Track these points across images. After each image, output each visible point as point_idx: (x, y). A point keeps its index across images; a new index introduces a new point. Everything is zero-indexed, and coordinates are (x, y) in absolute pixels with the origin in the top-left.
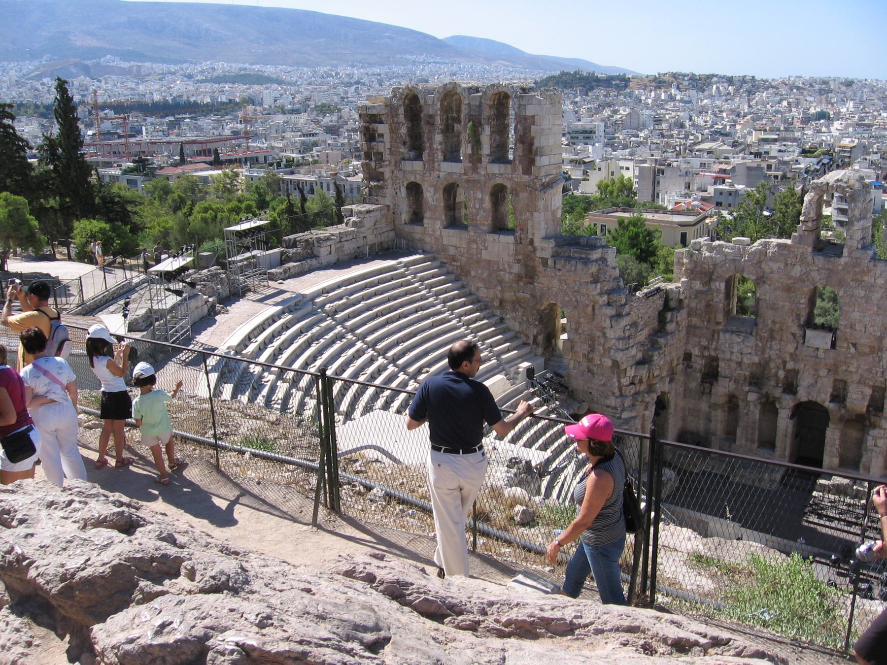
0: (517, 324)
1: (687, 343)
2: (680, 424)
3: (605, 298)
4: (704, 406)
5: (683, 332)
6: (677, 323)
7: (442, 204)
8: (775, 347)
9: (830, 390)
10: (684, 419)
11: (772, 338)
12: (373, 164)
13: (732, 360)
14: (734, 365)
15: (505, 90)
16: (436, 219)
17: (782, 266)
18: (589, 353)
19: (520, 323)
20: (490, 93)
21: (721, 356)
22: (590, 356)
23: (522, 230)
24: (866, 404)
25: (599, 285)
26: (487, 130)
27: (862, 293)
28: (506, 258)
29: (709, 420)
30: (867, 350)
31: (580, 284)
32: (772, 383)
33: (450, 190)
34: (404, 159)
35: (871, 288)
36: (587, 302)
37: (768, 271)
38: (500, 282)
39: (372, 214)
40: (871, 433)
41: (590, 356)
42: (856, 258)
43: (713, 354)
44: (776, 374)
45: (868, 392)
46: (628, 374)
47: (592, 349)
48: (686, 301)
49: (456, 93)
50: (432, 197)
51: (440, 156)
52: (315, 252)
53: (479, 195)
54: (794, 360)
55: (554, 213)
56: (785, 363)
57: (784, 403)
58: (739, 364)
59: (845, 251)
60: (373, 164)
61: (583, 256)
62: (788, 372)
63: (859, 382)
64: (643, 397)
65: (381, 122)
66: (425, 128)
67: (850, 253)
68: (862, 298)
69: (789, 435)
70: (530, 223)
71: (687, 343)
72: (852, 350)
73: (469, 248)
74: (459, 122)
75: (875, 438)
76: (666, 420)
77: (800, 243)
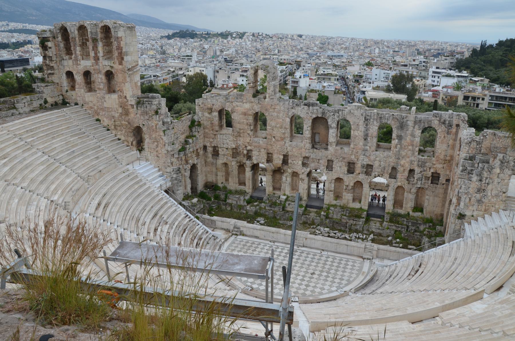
0: (123, 136)
1: (204, 141)
2: (204, 178)
3: (161, 122)
4: (214, 170)
5: (202, 136)
6: (198, 132)
7: (84, 81)
9: (266, 157)
10: (206, 176)
12: (48, 62)
13: (223, 147)
14: (225, 150)
15: (107, 24)
16: (81, 88)
19: (124, 136)
20: (100, 26)
21: (219, 146)
23: (121, 92)
24: (281, 162)
25: (158, 116)
26: (100, 45)
27: (276, 114)
28: (115, 106)
29: (217, 175)
30: (279, 139)
32: (242, 156)
33: (87, 74)
34: (63, 59)
35: (279, 112)
36: (153, 124)
38: (113, 117)
39: (49, 87)
43: (216, 145)
44: (243, 152)
45: (282, 157)
46: (175, 156)
47: (157, 146)
48: (202, 122)
49: (85, 27)
50: (79, 78)
51: (80, 57)
52: (16, 107)
53: (100, 76)
54: (250, 146)
55: (136, 83)
56: (246, 147)
57: (247, 164)
58: (227, 149)
59: (267, 96)
60: (48, 62)
62: (248, 151)
64: (183, 167)
65: (49, 41)
66: (72, 44)
70: (124, 89)
71: (204, 141)
72: (274, 140)
73: (98, 101)
74: (88, 41)
75: (286, 177)
76: (197, 176)
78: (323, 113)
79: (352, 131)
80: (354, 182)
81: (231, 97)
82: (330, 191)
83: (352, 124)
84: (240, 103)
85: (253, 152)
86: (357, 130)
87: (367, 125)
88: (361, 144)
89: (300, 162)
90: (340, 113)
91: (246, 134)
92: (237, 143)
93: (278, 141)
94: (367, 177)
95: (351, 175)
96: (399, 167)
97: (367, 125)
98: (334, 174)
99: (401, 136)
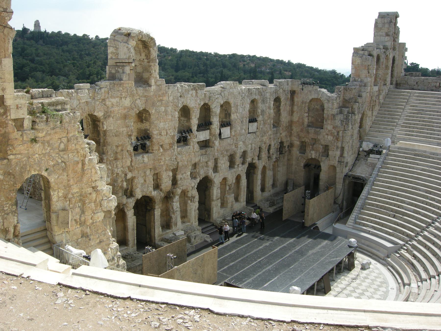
8: (119, 166)
11: (116, 159)
17: (118, 99)
18: (80, 216)
22: (83, 219)
31: (68, 141)
36: (76, 159)
37: (110, 106)
40: (174, 200)
41: (83, 219)
42: (158, 86)
44: (122, 187)
45: (171, 174)
56: (126, 175)
61: (59, 107)
63: (166, 170)
67: (155, 83)
68: (163, 112)
69: (135, 228)
72: (161, 150)
77: (129, 80)
78: (210, 97)
79: (232, 115)
80: (235, 177)
81: (103, 90)
82: (218, 199)
83: (232, 105)
84: (118, 99)
85: (136, 181)
86: (236, 112)
87: (243, 105)
88: (239, 128)
89: (189, 173)
90: (223, 94)
91: (125, 152)
92: (113, 173)
93: (167, 150)
94: (244, 166)
95: (234, 170)
96: (263, 145)
97: (243, 105)
98: (221, 175)
99: (264, 110)
